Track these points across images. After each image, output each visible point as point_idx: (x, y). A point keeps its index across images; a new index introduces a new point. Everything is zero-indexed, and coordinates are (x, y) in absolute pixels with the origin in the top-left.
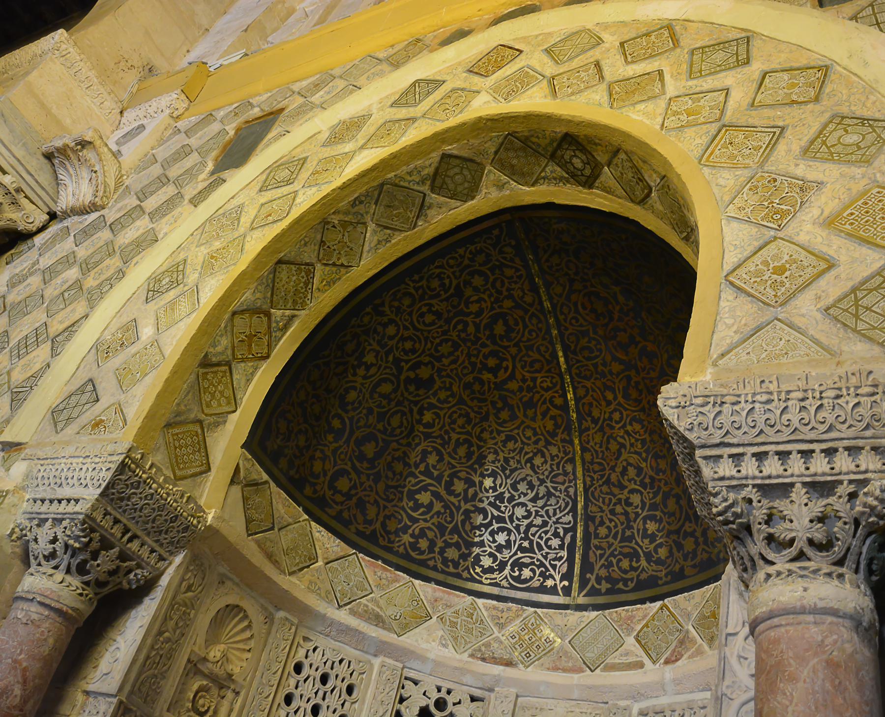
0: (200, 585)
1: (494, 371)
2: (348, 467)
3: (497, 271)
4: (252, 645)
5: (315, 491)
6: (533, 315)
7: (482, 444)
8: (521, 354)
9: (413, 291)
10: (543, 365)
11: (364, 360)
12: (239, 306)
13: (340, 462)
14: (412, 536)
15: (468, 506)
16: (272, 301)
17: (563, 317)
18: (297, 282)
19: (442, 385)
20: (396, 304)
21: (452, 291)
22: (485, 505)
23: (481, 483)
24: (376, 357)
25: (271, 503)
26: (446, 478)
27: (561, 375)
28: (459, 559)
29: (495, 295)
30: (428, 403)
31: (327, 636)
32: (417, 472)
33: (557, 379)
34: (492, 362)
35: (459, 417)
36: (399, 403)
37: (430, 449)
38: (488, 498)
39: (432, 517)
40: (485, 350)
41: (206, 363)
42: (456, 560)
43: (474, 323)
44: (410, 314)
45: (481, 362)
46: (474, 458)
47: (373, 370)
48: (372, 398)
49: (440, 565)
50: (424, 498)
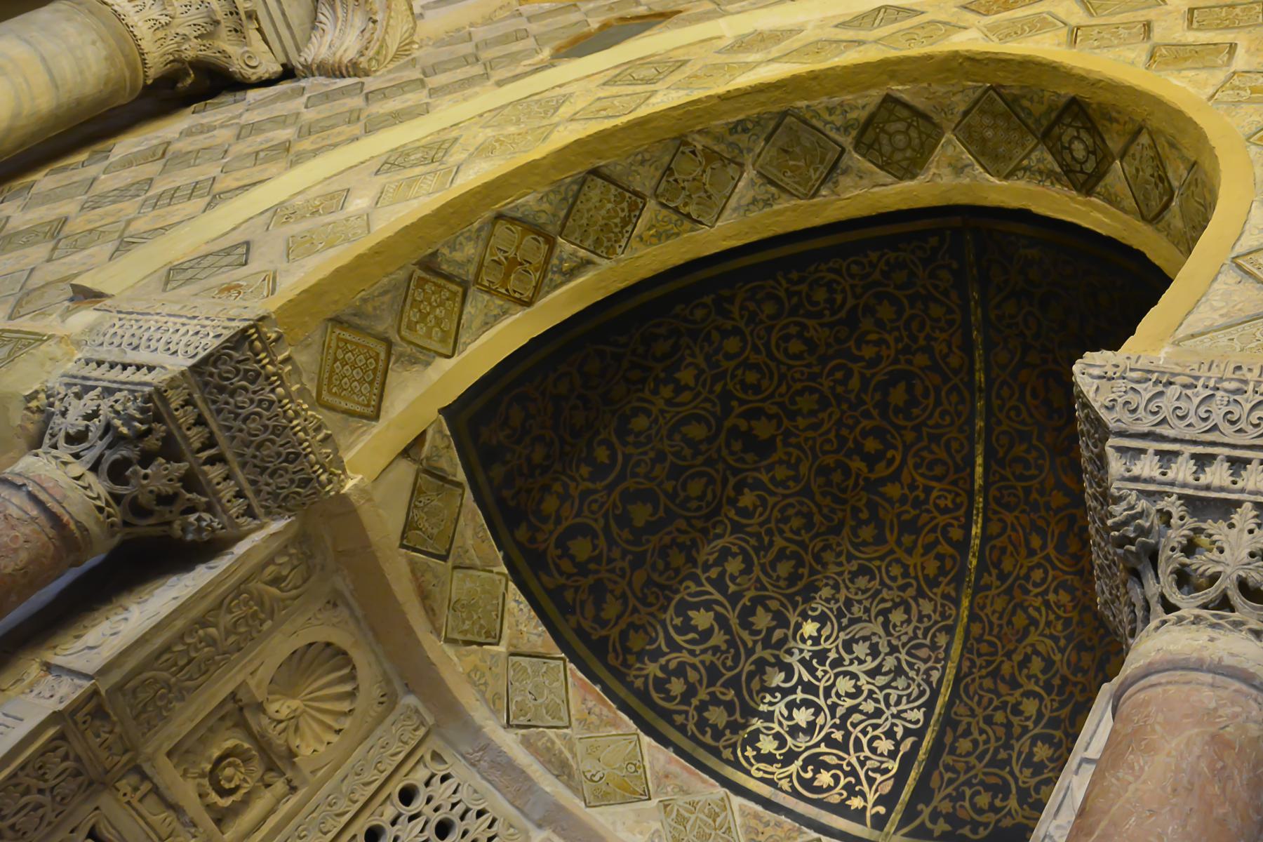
0: (296, 588)
6: (955, 388)
7: (819, 568)
9: (782, 294)
10: (948, 471)
11: (677, 375)
12: (511, 209)
14: (664, 668)
15: (767, 654)
18: (613, 214)
19: (785, 458)
20: (752, 306)
22: (794, 660)
23: (799, 626)
24: (697, 378)
26: (745, 601)
28: (726, 727)
29: (906, 340)
30: (755, 478)
32: (703, 578)
34: (871, 445)
35: (797, 514)
36: (709, 462)
37: (735, 549)
38: (801, 651)
39: (704, 652)
40: (865, 423)
41: (430, 265)
42: (721, 726)
43: (862, 376)
44: (769, 329)
45: (855, 440)
46: (800, 585)
47: (686, 396)
48: (670, 437)
49: (691, 727)
50: (702, 619)
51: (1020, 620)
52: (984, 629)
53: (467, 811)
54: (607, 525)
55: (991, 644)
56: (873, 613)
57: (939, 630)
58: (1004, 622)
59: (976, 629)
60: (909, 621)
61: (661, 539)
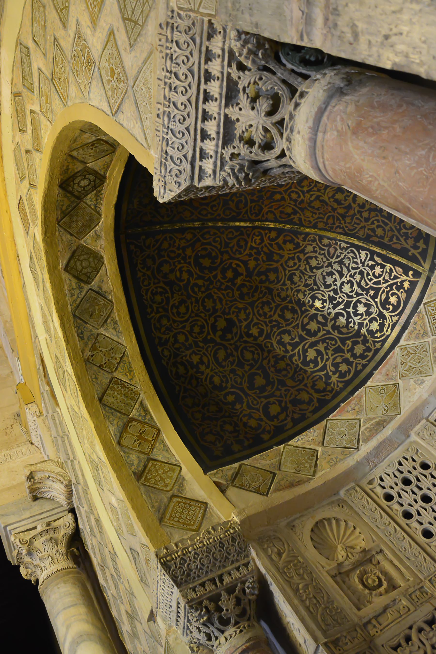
1: (237, 274)
2: (264, 401)
3: (162, 253)
4: (353, 524)
5: (269, 432)
7: (289, 299)
8: (230, 251)
9: (158, 315)
10: (242, 239)
11: (195, 363)
13: (258, 406)
16: (124, 414)
17: (209, 215)
19: (235, 314)
20: (163, 329)
21: (167, 288)
24: (196, 354)
25: (257, 468)
27: (254, 228)
29: (179, 259)
30: (245, 328)
31: (376, 466)
32: (291, 353)
33: (256, 231)
34: (230, 274)
35: (263, 309)
36: (236, 349)
37: (278, 338)
43: (196, 279)
44: (174, 321)
45: (227, 282)
46: (297, 308)
47: (205, 360)
48: (223, 367)
50: (311, 354)
51: (317, 204)
52: (320, 222)
53: (398, 470)
54: (263, 397)
55: (328, 218)
56: (311, 274)
57: (321, 243)
58: (318, 212)
59: (321, 225)
60: (316, 257)
61: (272, 372)
